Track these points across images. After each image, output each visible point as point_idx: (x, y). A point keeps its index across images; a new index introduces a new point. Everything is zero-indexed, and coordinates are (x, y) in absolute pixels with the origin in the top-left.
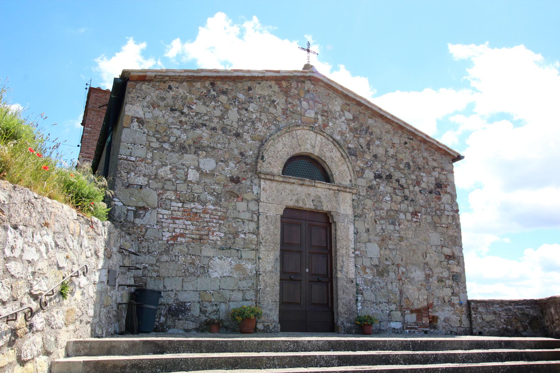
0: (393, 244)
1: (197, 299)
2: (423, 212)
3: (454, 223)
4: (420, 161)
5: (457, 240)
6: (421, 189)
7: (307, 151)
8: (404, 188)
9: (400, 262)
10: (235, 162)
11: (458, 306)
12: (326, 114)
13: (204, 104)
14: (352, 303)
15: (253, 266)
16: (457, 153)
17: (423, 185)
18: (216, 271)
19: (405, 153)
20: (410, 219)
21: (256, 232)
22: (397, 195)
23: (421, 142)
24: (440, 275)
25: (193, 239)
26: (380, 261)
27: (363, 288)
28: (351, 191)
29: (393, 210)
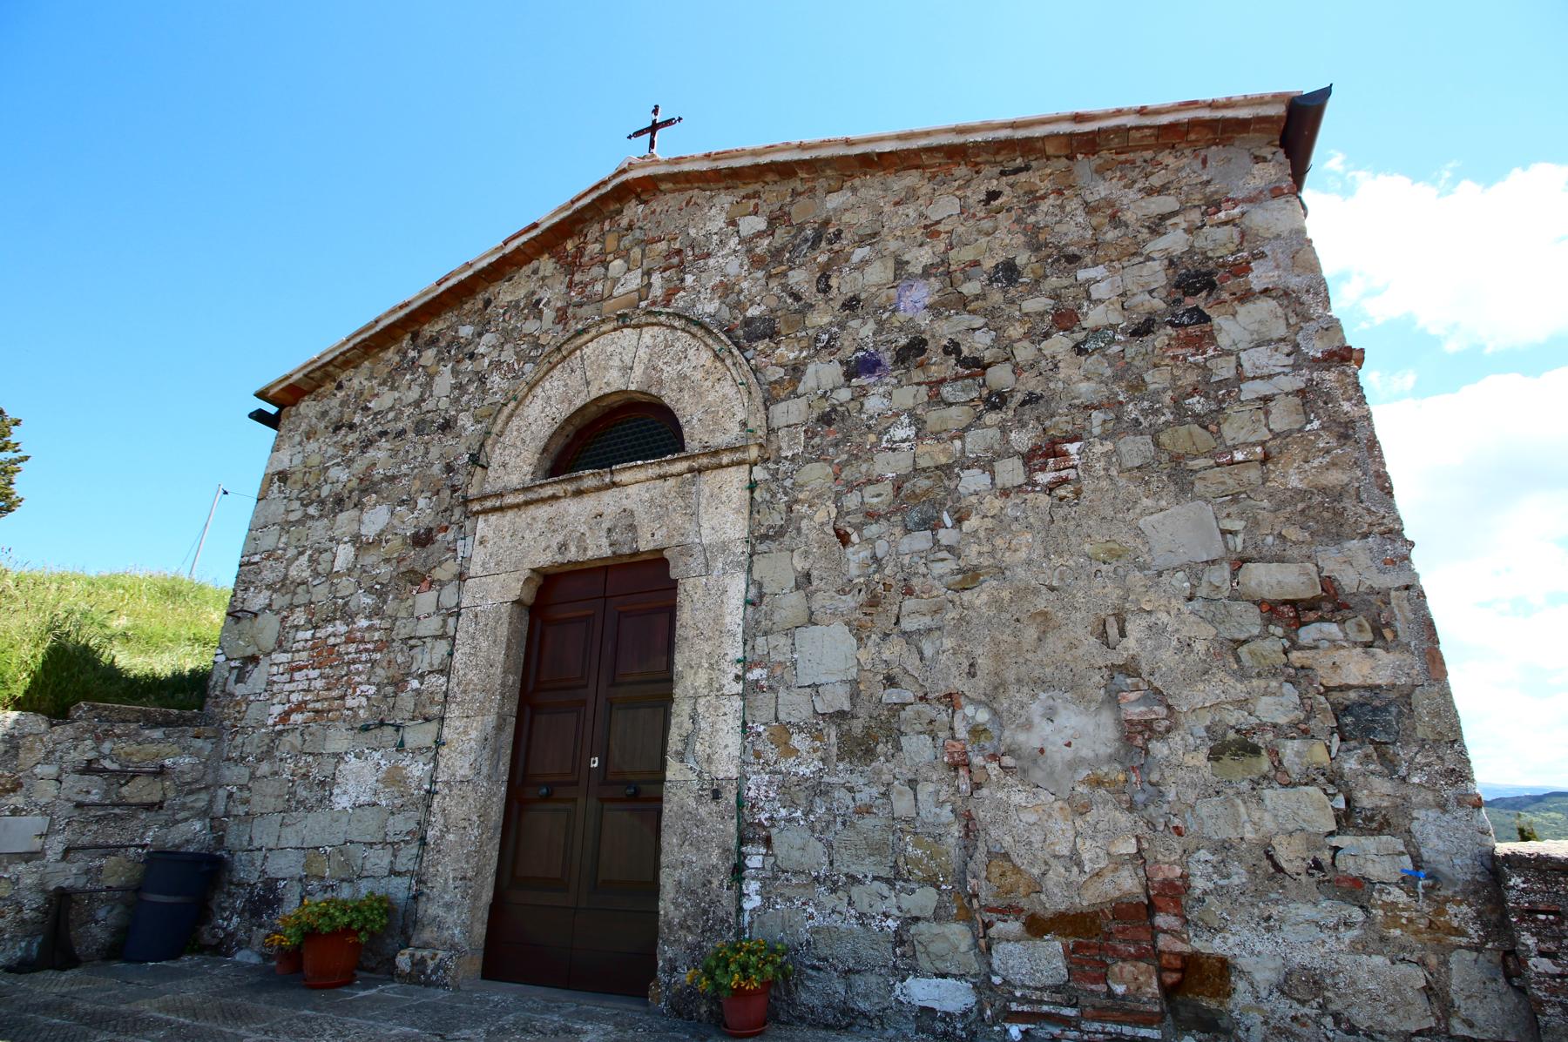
0: (924, 609)
1: (299, 871)
2: (1097, 431)
3: (1316, 424)
4: (1072, 229)
5: (1348, 503)
6: (1080, 336)
7: (608, 390)
8: (986, 367)
9: (958, 683)
10: (429, 494)
11: (1398, 895)
12: (675, 260)
13: (393, 388)
14: (716, 883)
15: (426, 768)
16: (1276, 98)
17: (1095, 317)
18: (345, 792)
19: (988, 234)
20: (1021, 479)
21: (445, 670)
22: (951, 404)
23: (1071, 157)
24: (1235, 717)
25: (317, 711)
26: (854, 696)
27: (771, 818)
28: (738, 456)
29: (924, 470)
